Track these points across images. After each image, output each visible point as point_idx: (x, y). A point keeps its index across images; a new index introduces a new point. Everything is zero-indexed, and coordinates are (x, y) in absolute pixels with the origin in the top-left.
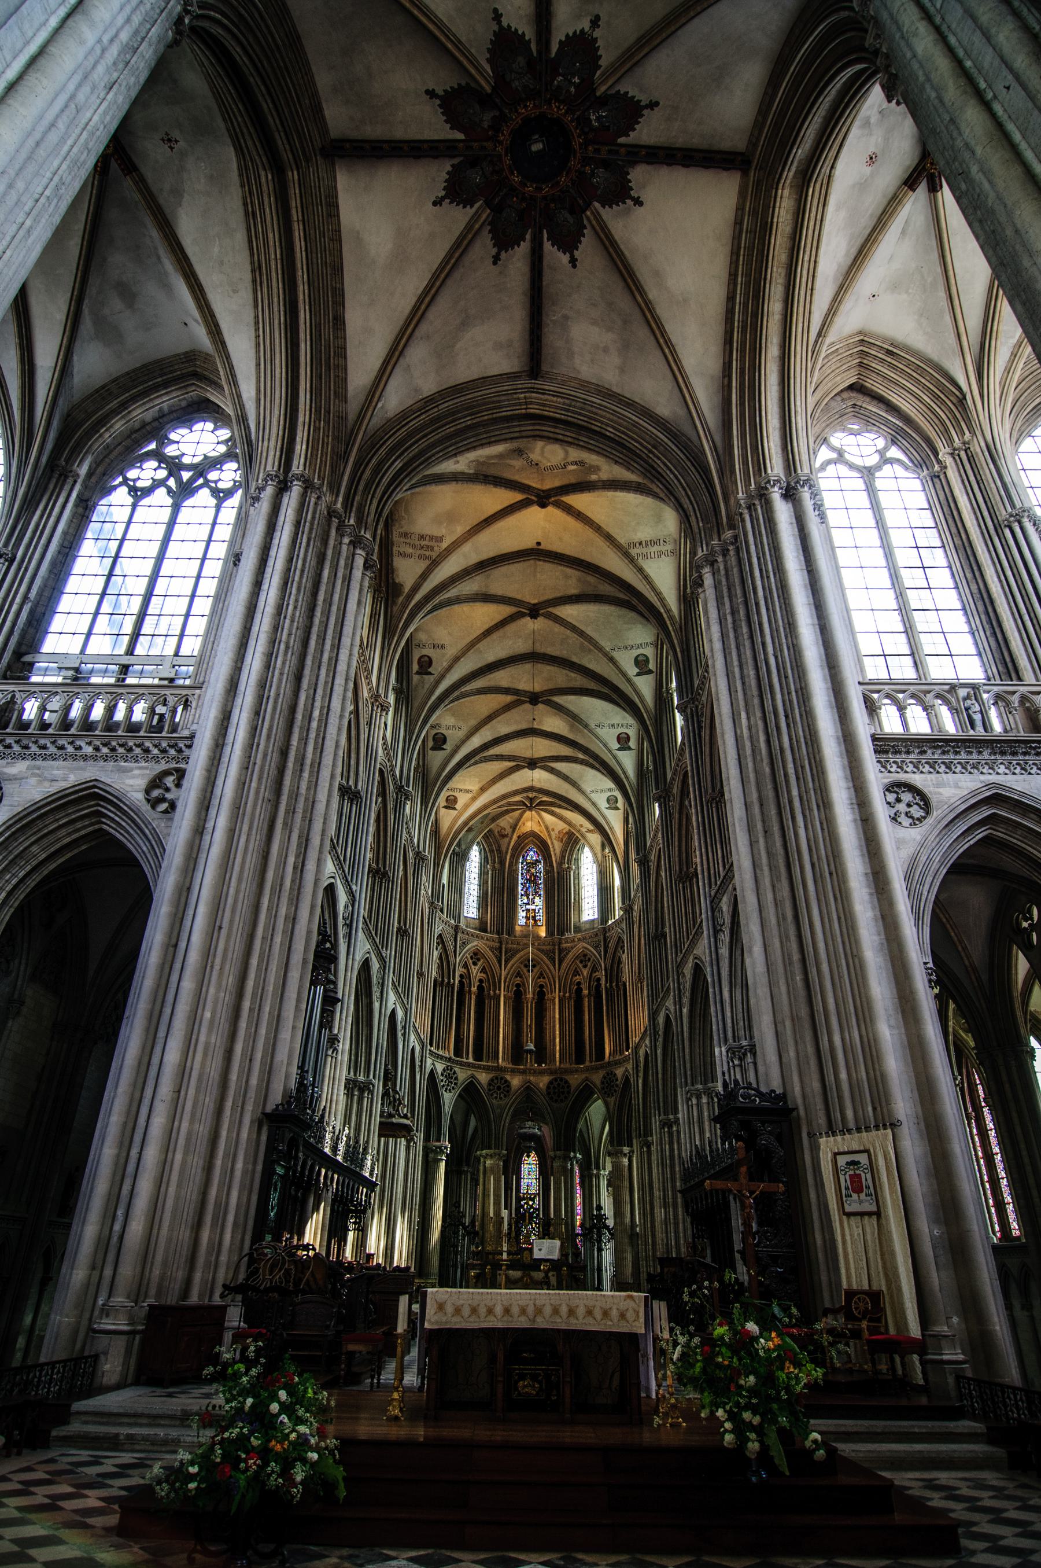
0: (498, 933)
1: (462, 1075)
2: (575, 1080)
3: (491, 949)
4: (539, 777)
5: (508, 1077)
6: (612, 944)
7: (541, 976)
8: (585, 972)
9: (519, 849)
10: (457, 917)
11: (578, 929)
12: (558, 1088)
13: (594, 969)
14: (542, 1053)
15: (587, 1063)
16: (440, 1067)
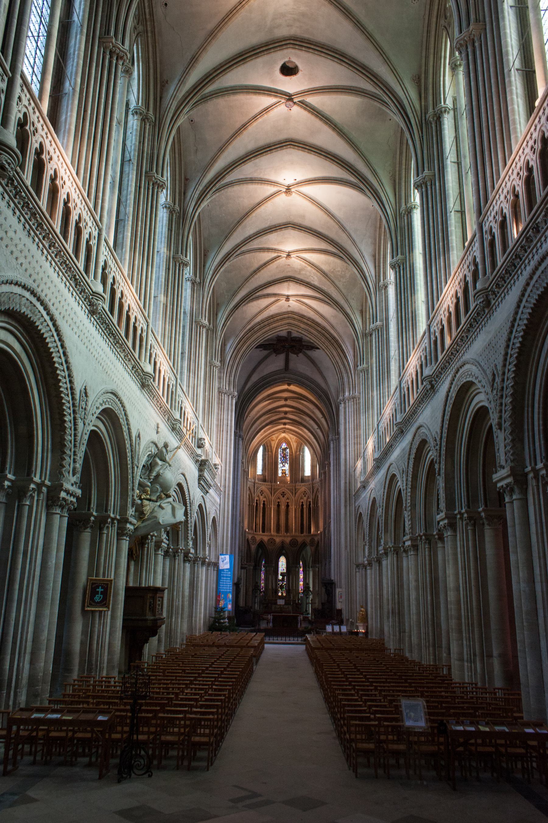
0: (271, 482)
1: (258, 538)
2: (300, 540)
3: (268, 489)
4: (287, 426)
5: (275, 538)
6: (315, 490)
7: (288, 499)
8: (305, 498)
9: (279, 445)
10: (254, 478)
11: (303, 480)
12: (294, 542)
13: (308, 498)
14: (287, 529)
15: (305, 533)
16: (250, 537)
